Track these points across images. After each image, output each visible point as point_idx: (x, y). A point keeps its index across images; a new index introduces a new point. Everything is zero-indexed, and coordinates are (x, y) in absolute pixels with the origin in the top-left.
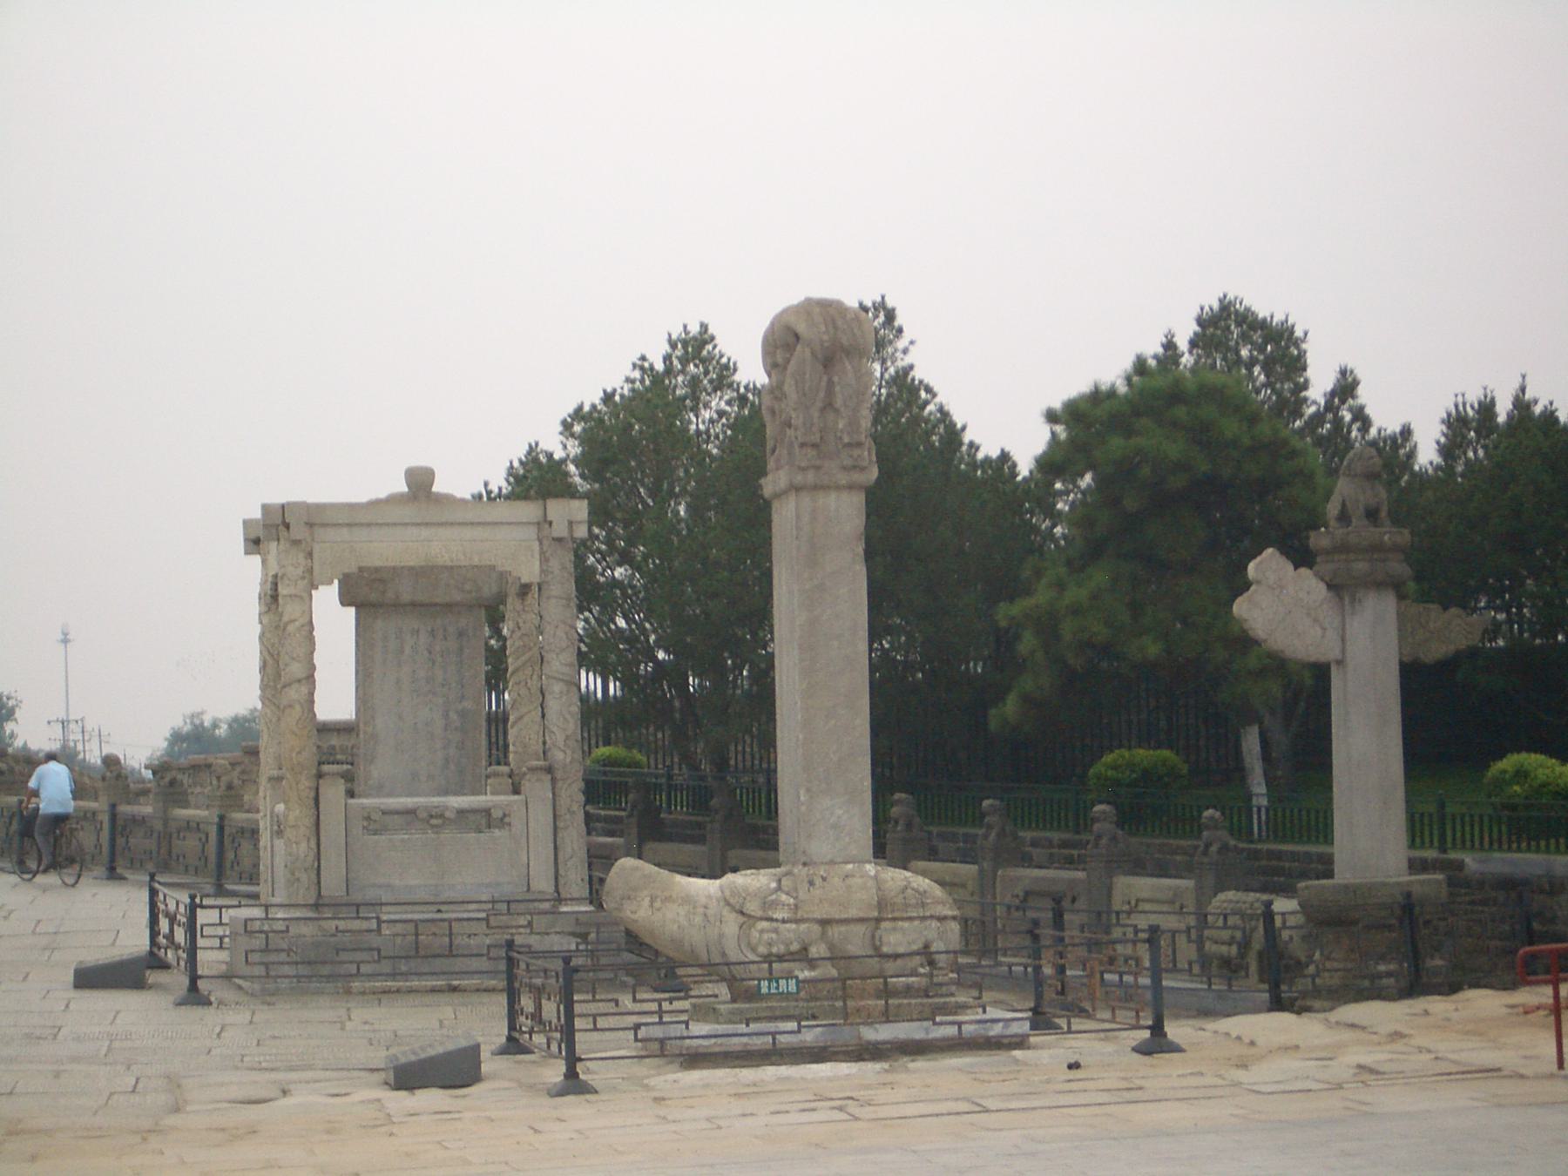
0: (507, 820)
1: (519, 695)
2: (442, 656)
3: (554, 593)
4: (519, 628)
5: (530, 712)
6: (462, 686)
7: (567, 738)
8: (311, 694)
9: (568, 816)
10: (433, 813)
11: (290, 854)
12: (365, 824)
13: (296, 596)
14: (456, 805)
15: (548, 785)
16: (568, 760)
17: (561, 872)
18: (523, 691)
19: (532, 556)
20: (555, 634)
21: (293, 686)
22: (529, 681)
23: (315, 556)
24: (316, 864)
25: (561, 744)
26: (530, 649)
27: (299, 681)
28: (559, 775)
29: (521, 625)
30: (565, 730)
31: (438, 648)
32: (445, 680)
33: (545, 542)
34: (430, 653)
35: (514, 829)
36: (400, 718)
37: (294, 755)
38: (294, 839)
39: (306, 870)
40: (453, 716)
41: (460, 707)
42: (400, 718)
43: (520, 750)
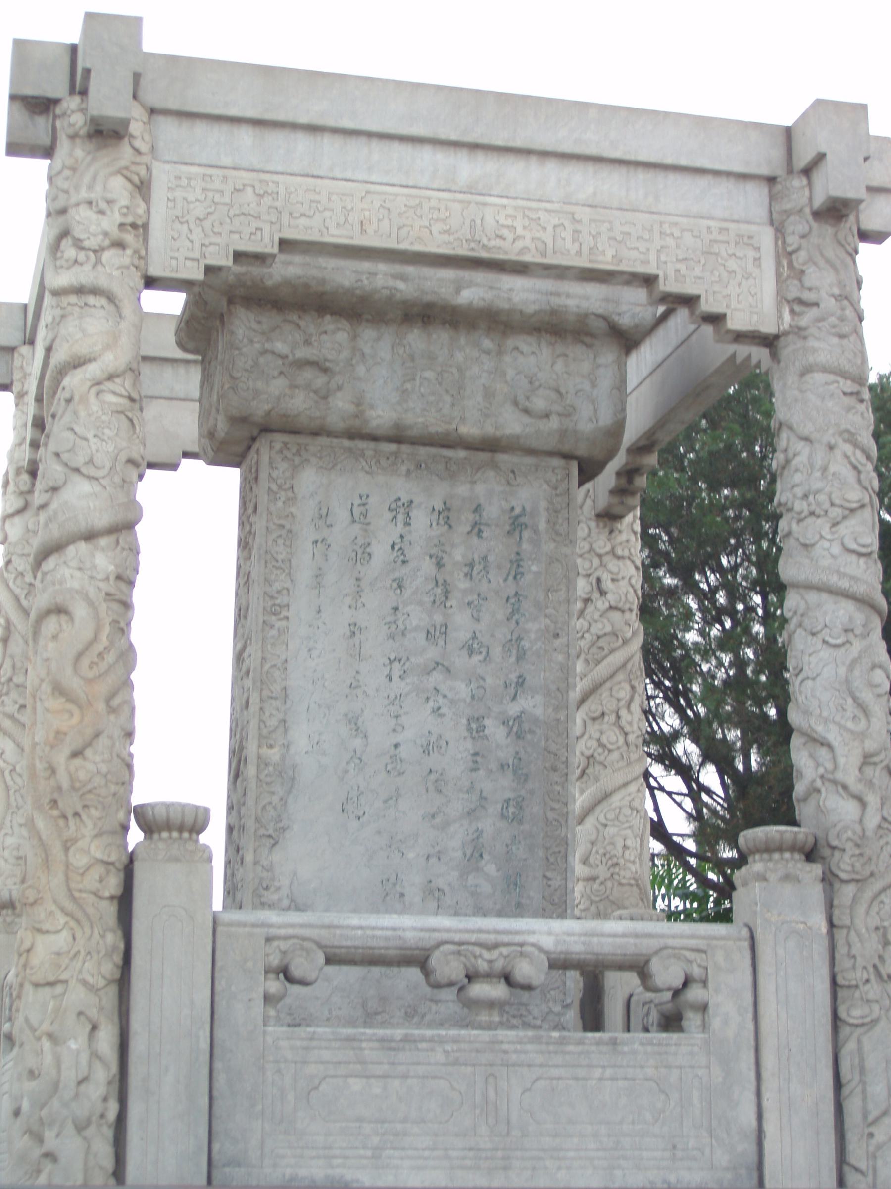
0: (695, 994)
1: (601, 744)
2: (469, 575)
3: (822, 358)
4: (603, 593)
5: (626, 785)
6: (520, 658)
7: (867, 759)
8: (126, 578)
9: (874, 990)
10: (483, 966)
11: (32, 1074)
12: (274, 986)
13: (95, 291)
14: (548, 942)
15: (816, 892)
16: (872, 821)
17: (857, 1154)
18: (612, 736)
19: (757, 260)
20: (824, 469)
21: (71, 550)
22: (624, 713)
23: (159, 193)
24: (113, 1109)
25: (849, 774)
26: (625, 642)
27: (90, 536)
28: (844, 864)
29: (607, 584)
30: (862, 736)
31: (458, 555)
32: (474, 637)
33: (797, 226)
34: (439, 565)
35: (716, 1023)
36: (354, 723)
37: (61, 758)
38: (46, 1027)
39: (80, 1128)
40: (496, 732)
41: (513, 709)
42: (354, 723)
43: (602, 872)
